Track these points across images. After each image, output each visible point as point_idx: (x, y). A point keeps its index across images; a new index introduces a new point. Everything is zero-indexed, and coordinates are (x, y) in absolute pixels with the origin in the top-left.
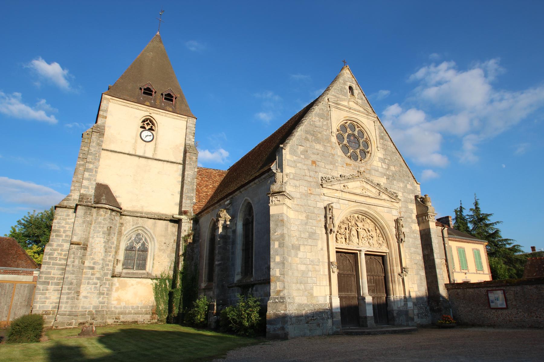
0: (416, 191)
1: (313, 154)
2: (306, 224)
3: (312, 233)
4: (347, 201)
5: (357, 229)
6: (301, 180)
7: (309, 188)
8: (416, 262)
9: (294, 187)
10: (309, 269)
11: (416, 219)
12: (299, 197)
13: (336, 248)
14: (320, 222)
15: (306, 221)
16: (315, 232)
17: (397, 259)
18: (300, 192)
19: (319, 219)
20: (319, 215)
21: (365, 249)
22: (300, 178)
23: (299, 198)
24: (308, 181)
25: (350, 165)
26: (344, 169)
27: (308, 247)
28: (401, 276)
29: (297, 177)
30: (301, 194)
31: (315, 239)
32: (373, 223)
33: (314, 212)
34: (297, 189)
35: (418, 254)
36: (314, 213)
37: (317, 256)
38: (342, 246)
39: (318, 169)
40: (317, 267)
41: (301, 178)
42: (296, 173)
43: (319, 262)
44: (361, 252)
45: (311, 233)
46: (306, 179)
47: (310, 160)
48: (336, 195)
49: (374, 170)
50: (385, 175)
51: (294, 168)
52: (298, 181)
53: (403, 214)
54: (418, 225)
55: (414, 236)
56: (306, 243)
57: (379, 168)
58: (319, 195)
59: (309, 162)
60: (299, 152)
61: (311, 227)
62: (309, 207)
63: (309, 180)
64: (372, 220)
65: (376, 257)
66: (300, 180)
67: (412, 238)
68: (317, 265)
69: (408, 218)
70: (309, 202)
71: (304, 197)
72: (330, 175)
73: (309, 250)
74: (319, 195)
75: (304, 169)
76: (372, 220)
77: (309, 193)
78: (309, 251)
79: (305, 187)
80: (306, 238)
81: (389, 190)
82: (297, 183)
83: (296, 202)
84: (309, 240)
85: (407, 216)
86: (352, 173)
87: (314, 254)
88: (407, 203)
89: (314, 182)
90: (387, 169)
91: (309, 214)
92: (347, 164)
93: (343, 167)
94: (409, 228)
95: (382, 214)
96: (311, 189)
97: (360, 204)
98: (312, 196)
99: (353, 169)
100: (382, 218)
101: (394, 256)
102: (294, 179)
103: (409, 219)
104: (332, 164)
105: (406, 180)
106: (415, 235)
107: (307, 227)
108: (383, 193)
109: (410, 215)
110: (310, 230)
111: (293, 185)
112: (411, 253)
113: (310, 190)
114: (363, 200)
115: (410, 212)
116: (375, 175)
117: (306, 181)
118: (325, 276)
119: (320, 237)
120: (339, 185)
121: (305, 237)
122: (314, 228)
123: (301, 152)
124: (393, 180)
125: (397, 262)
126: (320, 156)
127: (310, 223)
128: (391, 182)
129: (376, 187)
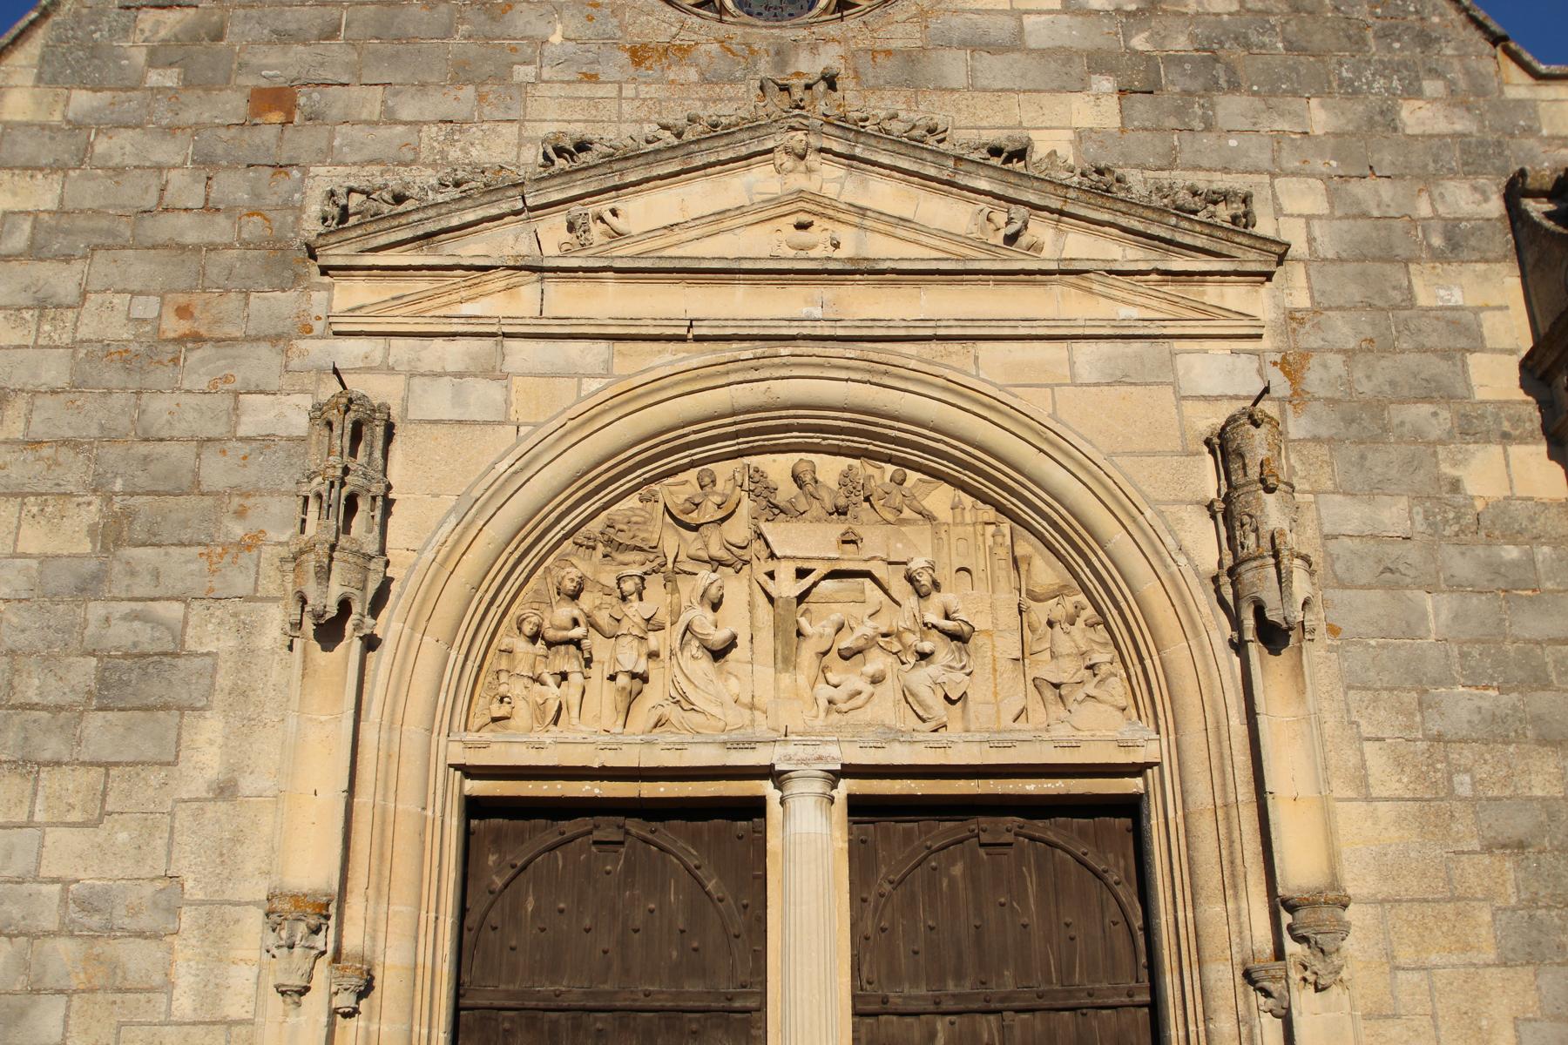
0: (1531, 142)
1: (283, 37)
2: (89, 586)
3: (143, 655)
4: (603, 345)
5: (764, 579)
6: (108, 248)
7: (182, 299)
8: (1520, 825)
9: (27, 315)
10: (39, 980)
11: (1520, 395)
12: (62, 382)
13: (470, 772)
14: (246, 558)
15: (92, 565)
16: (170, 647)
17: (1228, 817)
18: (75, 344)
19: (238, 530)
20: (247, 495)
21: (823, 751)
22: (96, 240)
23: (54, 392)
24: (183, 247)
25: (679, 52)
26: (611, 90)
27: (72, 785)
28: (1267, 994)
29: (67, 232)
30: (82, 353)
31: (166, 707)
32: (990, 513)
33: (197, 483)
34: (47, 327)
35: (1543, 741)
36: (195, 487)
37: (162, 851)
38: (539, 747)
39: (304, 141)
40: (136, 957)
41: (110, 233)
42: (69, 206)
43: (173, 911)
44: (794, 787)
45: (126, 656)
46: (162, 237)
47: (240, 88)
48: (468, 309)
49: (963, 44)
50: (1098, 62)
51: (58, 177)
52: (78, 266)
53: (1342, 371)
54: (1551, 456)
55: (1495, 568)
56: (52, 747)
57: (1028, 20)
58: (276, 339)
59: (232, 104)
60: (140, 56)
61: (134, 605)
62: (143, 449)
63: (191, 238)
64: (966, 477)
65: (1041, 827)
66: (99, 254)
67: (1456, 586)
68: (140, 934)
69: (1402, 401)
70: (158, 406)
71: (114, 376)
72: (433, 165)
73: (72, 807)
74: (276, 339)
75: (159, 168)
76: (966, 477)
77: (171, 335)
78: (76, 816)
79: (133, 293)
80: (59, 708)
81: (1138, 182)
82: (62, 280)
83: (21, 425)
84: (95, 722)
85: (1392, 383)
86: (677, 117)
87: (123, 836)
88: (1394, 272)
89: (246, 245)
90: (1129, 14)
91: (131, 501)
92: (638, 55)
93: (592, 78)
94: (1418, 498)
95: (1036, 403)
96: (197, 299)
97: (761, 348)
98: (207, 350)
99: (705, 80)
100: (1047, 439)
101: (1201, 794)
102: (35, 252)
103: (1426, 409)
104: (470, 81)
105: (1386, 69)
106: (1511, 553)
107: (96, 610)
108: (1061, 213)
109: (1438, 366)
110: (122, 634)
111: (22, 299)
112: (1439, 738)
113: (183, 312)
114: (803, 311)
115: (1432, 340)
116: (972, 87)
117: (154, 247)
118: (219, 1030)
119: (223, 681)
120: (511, 228)
121: (51, 699)
122: (174, 610)
123: (152, 53)
124: (1212, 87)
125: (1231, 843)
126: (351, 43)
127: (133, 574)
128: (1180, 112)
129: (961, 180)
